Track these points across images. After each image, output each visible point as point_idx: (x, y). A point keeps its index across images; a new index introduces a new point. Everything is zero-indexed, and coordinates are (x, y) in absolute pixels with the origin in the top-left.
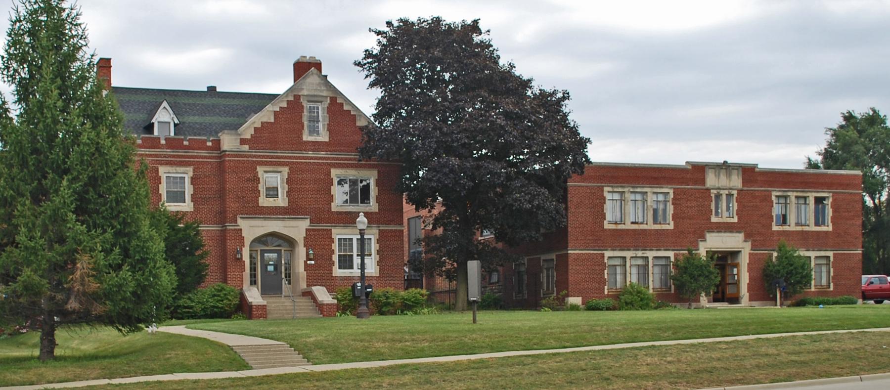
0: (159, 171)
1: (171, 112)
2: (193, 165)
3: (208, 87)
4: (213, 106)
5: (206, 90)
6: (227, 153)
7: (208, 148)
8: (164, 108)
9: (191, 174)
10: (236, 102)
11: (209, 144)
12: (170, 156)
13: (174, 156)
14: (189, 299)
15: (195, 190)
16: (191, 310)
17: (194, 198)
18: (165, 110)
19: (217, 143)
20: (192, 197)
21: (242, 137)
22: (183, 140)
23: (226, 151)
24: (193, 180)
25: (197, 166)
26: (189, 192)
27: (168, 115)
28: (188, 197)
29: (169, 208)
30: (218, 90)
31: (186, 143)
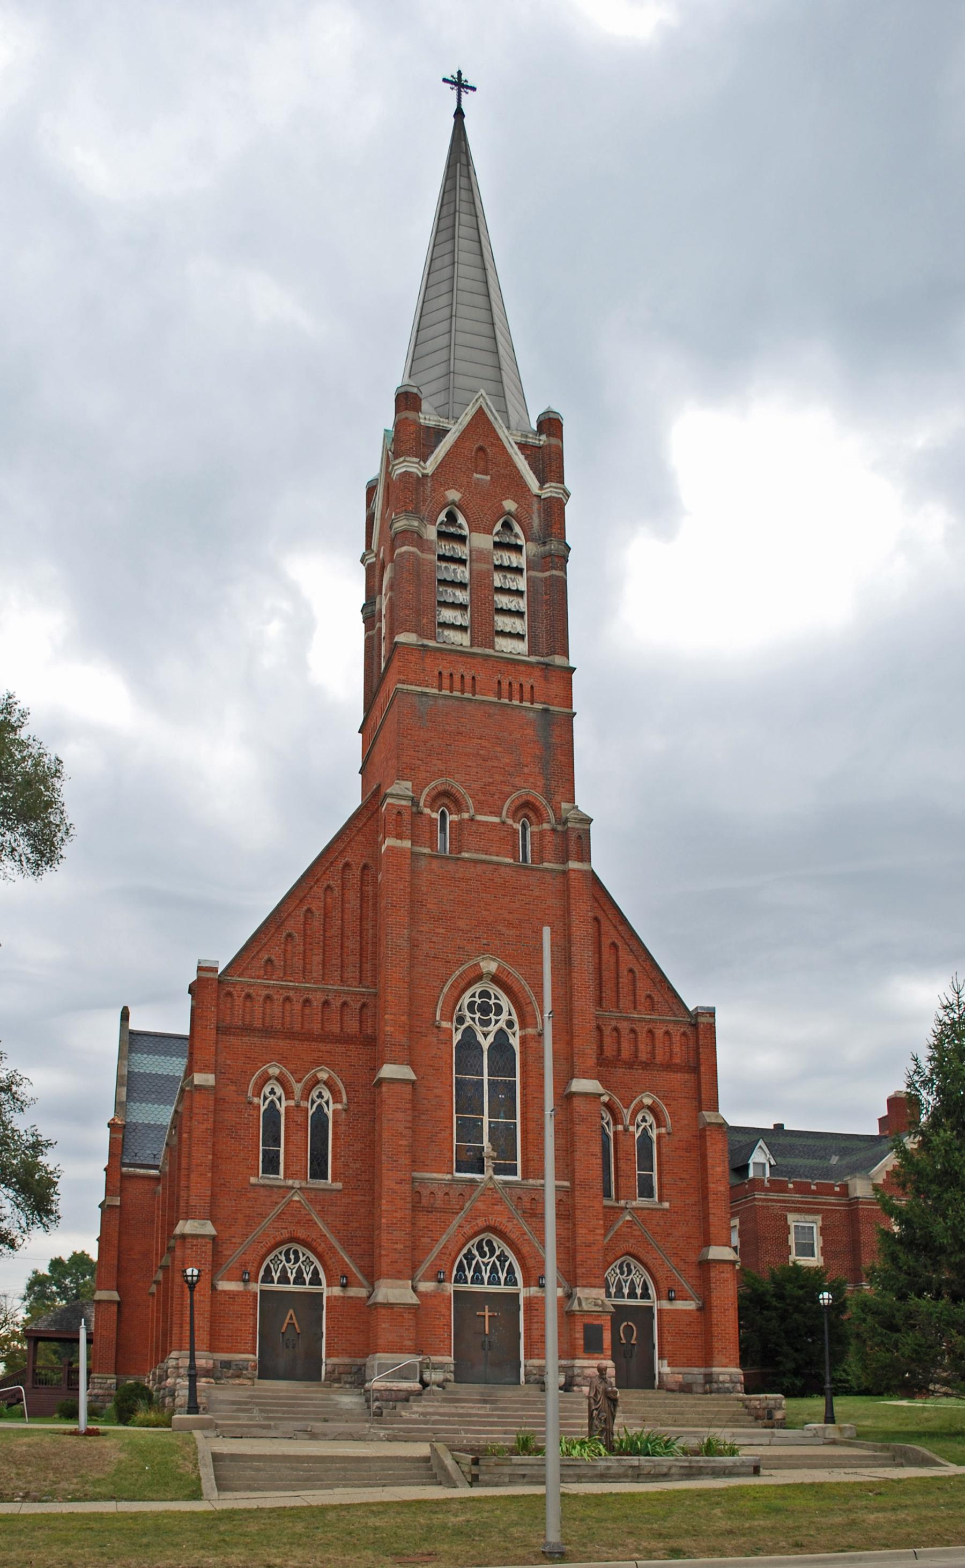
0: (788, 1219)
1: (767, 1152)
2: (822, 1213)
3: (774, 1125)
4: (790, 1146)
5: (772, 1127)
6: (860, 1200)
7: (836, 1194)
8: (760, 1147)
9: (820, 1224)
10: (810, 1142)
11: (837, 1189)
12: (798, 1202)
13: (802, 1202)
14: (844, 1371)
15: (824, 1241)
16: (847, 1385)
17: (824, 1252)
18: (760, 1150)
19: (845, 1187)
20: (822, 1250)
21: (874, 1182)
22: (810, 1184)
23: (859, 1198)
24: (823, 1230)
25: (826, 1215)
26: (818, 1244)
27: (764, 1155)
28: (817, 1250)
29: (799, 1263)
30: (786, 1128)
31: (813, 1187)
